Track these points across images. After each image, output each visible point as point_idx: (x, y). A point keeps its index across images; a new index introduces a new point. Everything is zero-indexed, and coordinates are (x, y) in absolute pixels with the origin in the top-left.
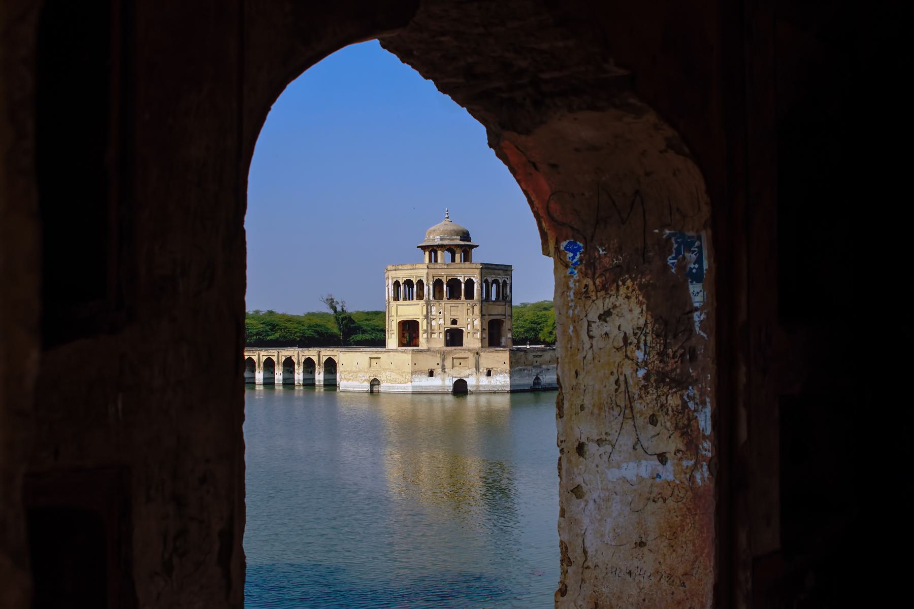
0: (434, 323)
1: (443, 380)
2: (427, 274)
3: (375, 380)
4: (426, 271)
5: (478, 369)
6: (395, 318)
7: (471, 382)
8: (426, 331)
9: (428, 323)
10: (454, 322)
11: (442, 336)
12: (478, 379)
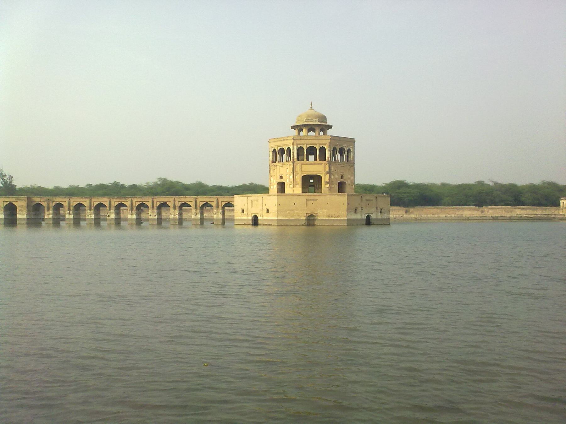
0: (332, 177)
1: (361, 215)
2: (330, 143)
3: (312, 215)
4: (329, 141)
5: (377, 208)
6: (300, 173)
7: (373, 216)
8: (327, 183)
9: (330, 177)
10: (342, 177)
11: (336, 187)
12: (377, 215)
